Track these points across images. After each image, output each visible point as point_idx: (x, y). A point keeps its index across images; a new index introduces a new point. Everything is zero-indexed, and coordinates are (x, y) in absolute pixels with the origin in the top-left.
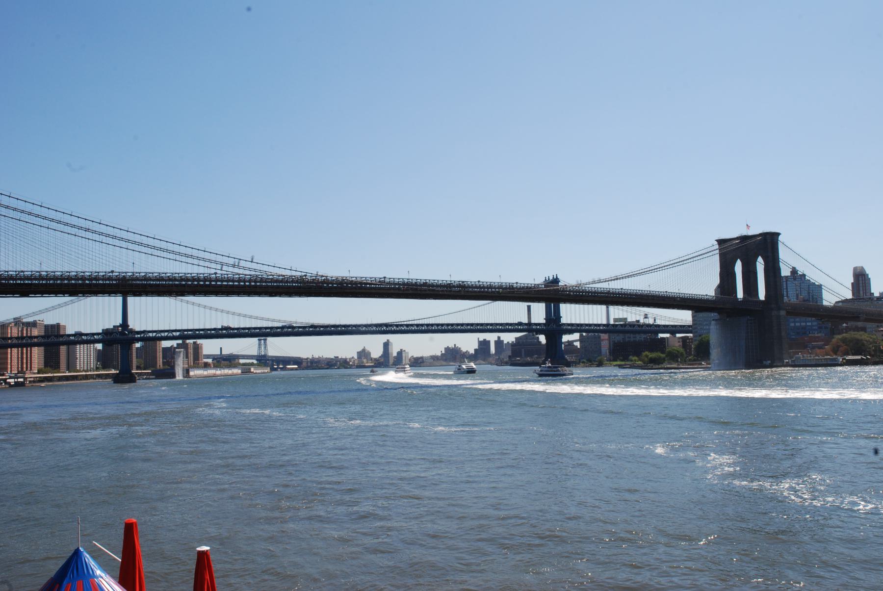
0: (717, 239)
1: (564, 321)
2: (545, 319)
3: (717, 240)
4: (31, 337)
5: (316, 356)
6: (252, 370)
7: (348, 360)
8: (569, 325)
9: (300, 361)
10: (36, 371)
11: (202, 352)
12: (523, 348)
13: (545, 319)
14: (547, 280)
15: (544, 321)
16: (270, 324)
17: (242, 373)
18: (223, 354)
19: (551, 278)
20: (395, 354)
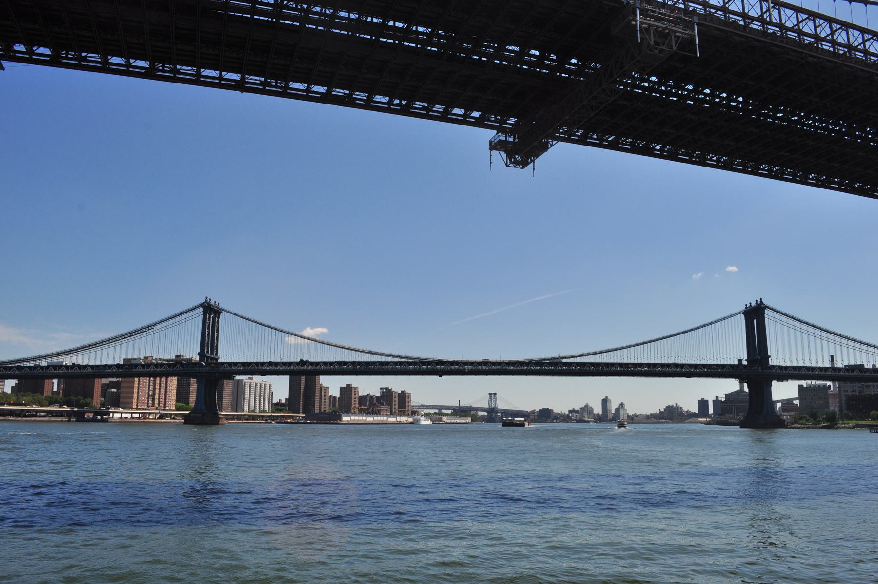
1: (773, 362)
6: (444, 419)
8: (781, 367)
11: (409, 402)
12: (734, 405)
14: (748, 305)
18: (461, 405)
19: (754, 304)
20: (613, 411)
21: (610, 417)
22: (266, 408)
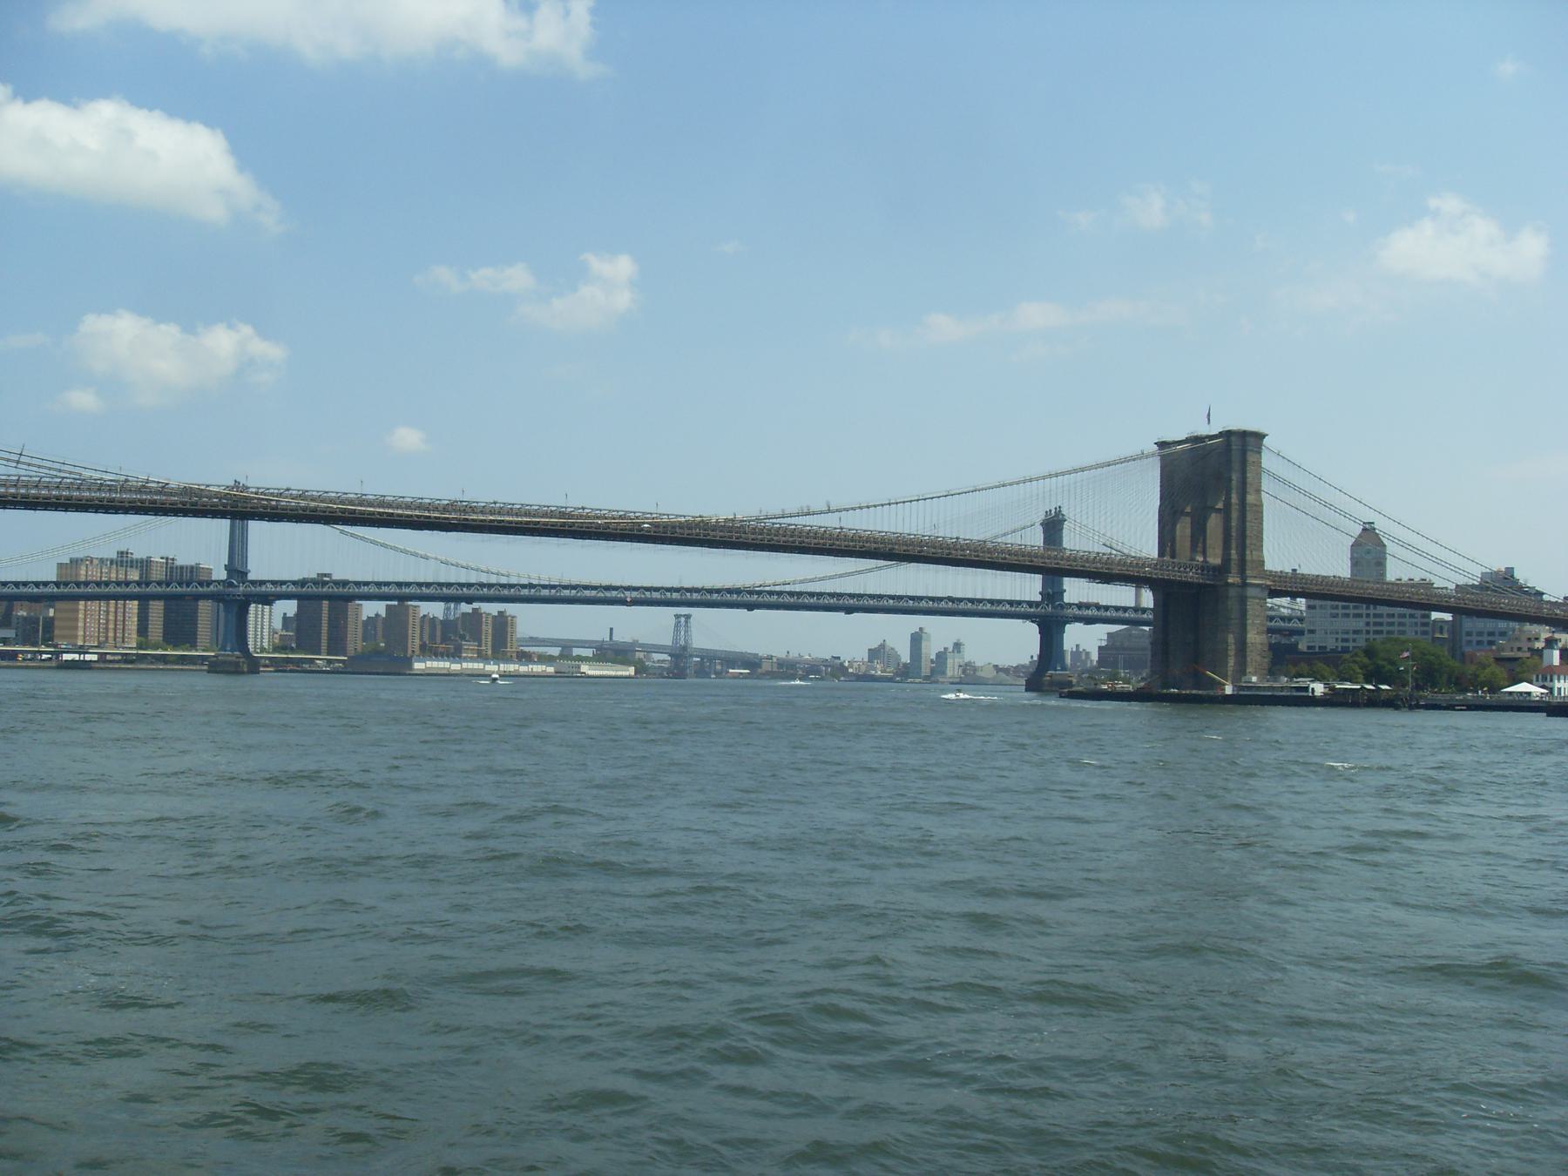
0: (1156, 441)
2: (1040, 593)
3: (1156, 443)
4: (127, 584)
5: (794, 655)
7: (846, 664)
8: (1080, 606)
9: (757, 661)
10: (135, 646)
13: (1040, 593)
15: (1039, 598)
16: (484, 579)
17: (556, 672)
18: (614, 639)
21: (925, 671)
22: (266, 645)
